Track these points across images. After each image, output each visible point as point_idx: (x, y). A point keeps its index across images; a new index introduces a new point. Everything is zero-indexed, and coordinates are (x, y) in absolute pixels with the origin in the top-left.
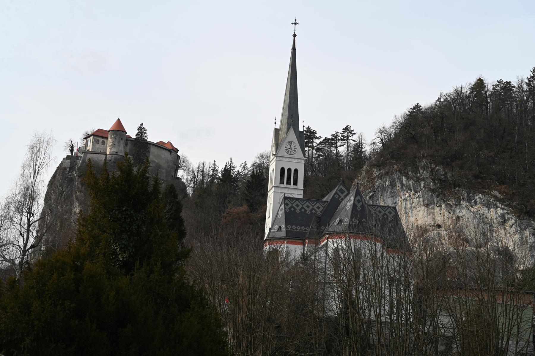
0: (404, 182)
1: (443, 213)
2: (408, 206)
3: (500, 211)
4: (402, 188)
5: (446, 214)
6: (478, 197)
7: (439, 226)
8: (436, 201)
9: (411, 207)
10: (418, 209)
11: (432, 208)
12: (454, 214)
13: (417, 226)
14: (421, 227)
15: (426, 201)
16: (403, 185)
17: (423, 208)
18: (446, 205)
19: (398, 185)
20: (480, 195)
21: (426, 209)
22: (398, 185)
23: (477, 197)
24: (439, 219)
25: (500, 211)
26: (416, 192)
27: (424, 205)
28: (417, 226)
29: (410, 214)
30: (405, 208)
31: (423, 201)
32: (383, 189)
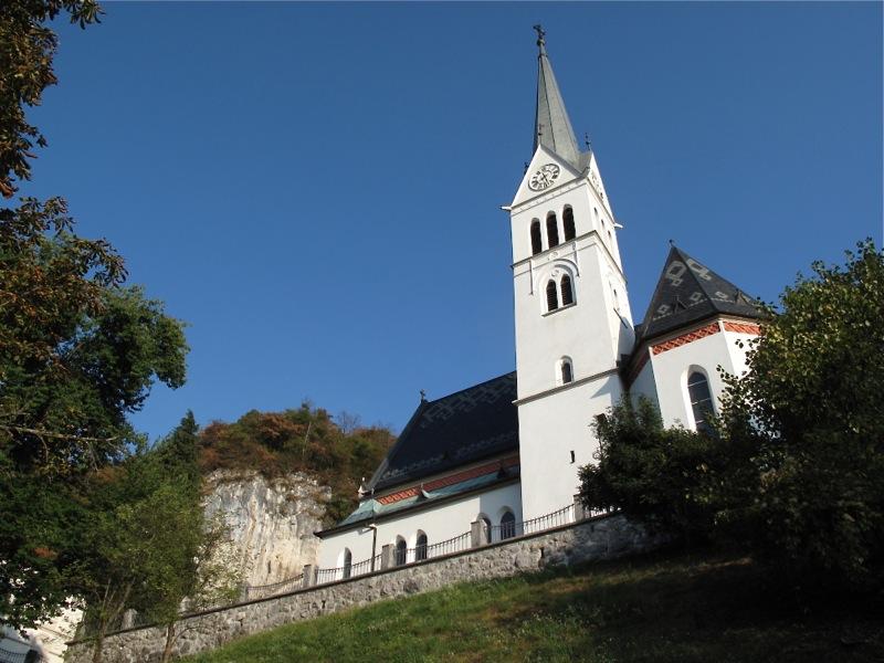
0: (268, 497)
2: (267, 533)
4: (261, 505)
9: (271, 538)
10: (286, 541)
11: (311, 543)
13: (280, 566)
14: (287, 569)
15: (303, 531)
16: (263, 500)
19: (254, 499)
21: (300, 542)
22: (254, 499)
26: (283, 513)
27: (297, 535)
28: (280, 566)
29: (268, 547)
30: (260, 535)
31: (298, 530)
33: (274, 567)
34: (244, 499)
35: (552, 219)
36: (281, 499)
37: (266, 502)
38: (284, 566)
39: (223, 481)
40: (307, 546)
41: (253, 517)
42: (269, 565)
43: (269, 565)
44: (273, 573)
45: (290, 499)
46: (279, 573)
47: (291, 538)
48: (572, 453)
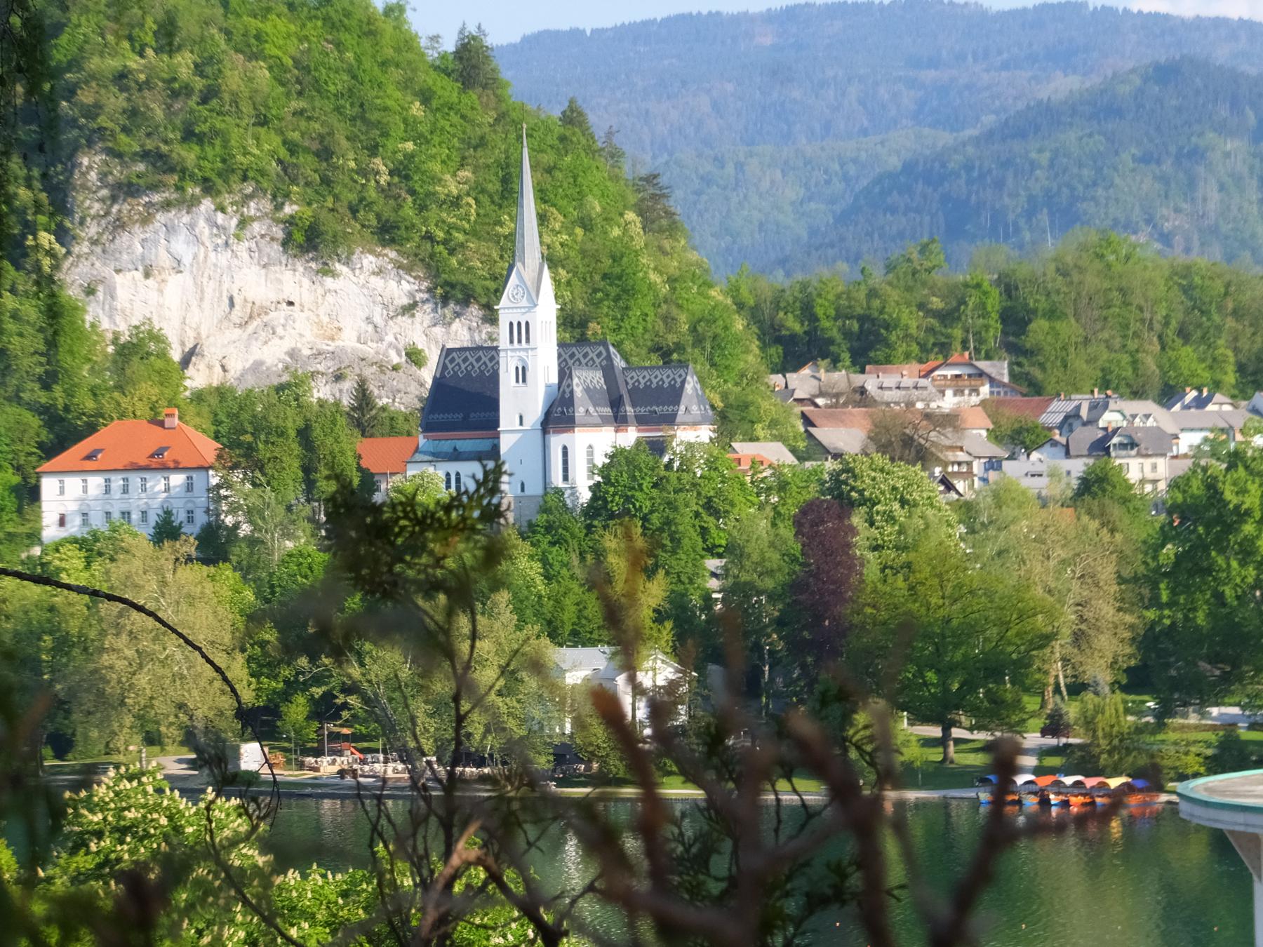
1: (300, 282)
3: (406, 286)
4: (211, 229)
5: (306, 282)
6: (369, 261)
7: (291, 303)
8: (284, 262)
9: (229, 267)
10: (245, 270)
12: (322, 284)
13: (245, 300)
16: (213, 224)
17: (256, 269)
18: (305, 269)
19: (202, 223)
20: (371, 258)
21: (263, 271)
23: (365, 262)
24: (290, 291)
25: (406, 286)
32: (170, 229)
33: (237, 300)
34: (191, 227)
35: (519, 324)
36: (234, 222)
37: (218, 227)
38: (250, 300)
39: (167, 205)
40: (272, 276)
41: (203, 244)
42: (231, 299)
43: (231, 299)
44: (237, 307)
45: (243, 223)
46: (244, 306)
47: (253, 267)
48: (521, 417)
